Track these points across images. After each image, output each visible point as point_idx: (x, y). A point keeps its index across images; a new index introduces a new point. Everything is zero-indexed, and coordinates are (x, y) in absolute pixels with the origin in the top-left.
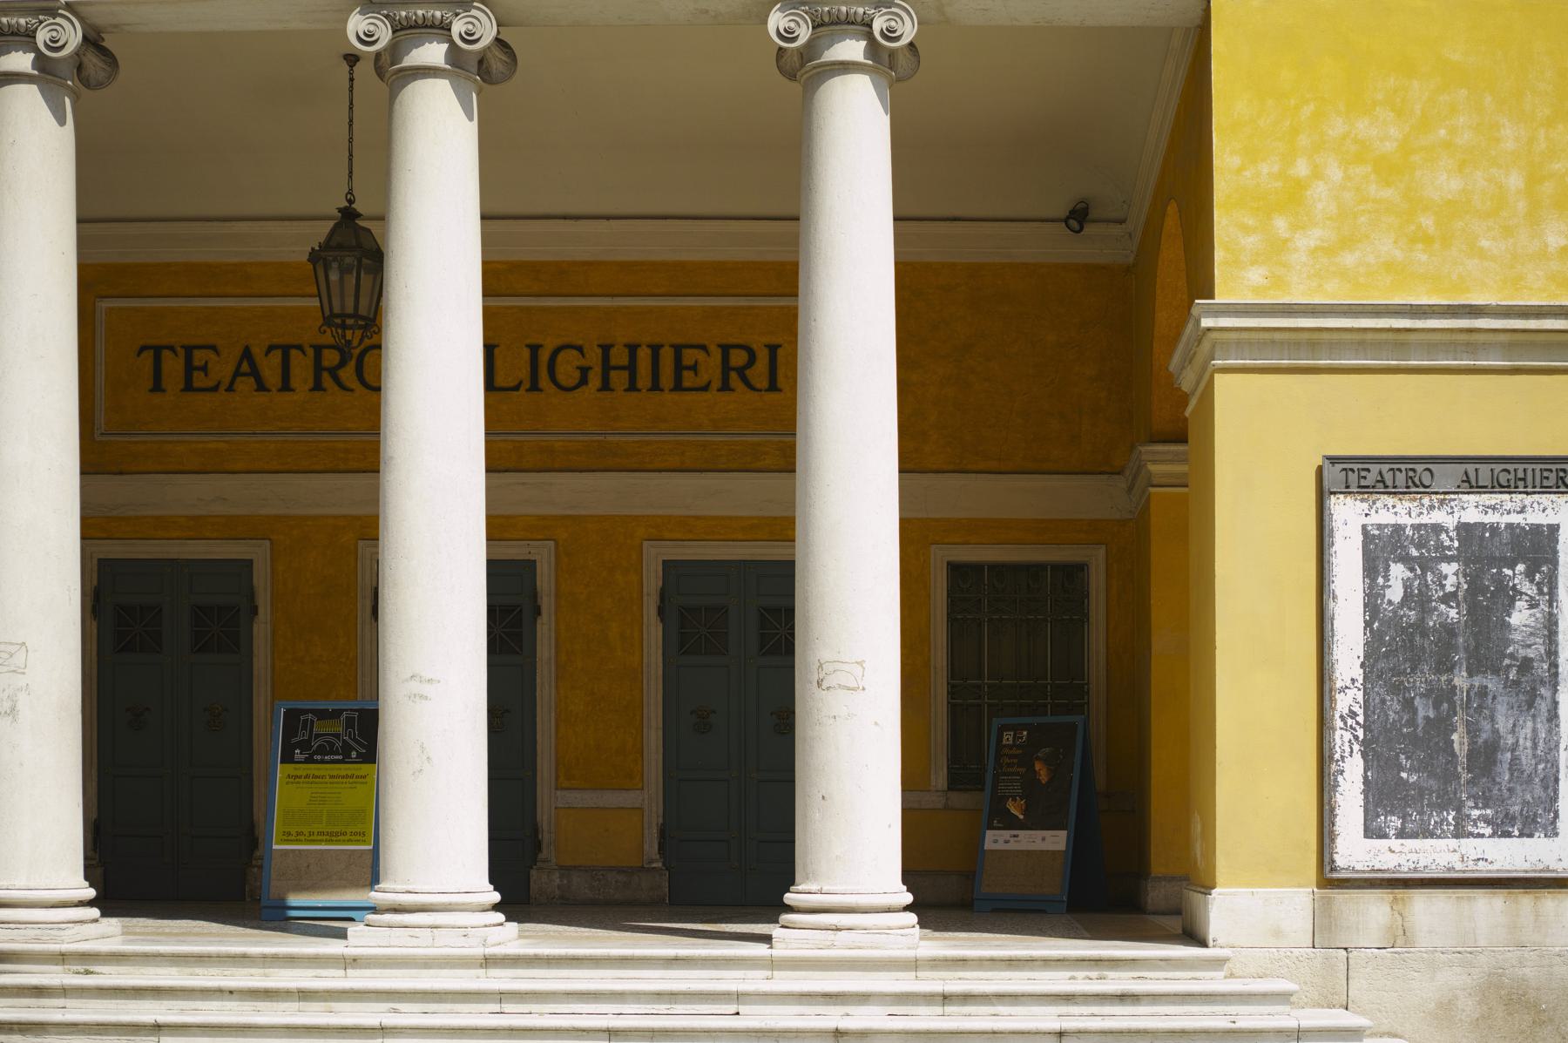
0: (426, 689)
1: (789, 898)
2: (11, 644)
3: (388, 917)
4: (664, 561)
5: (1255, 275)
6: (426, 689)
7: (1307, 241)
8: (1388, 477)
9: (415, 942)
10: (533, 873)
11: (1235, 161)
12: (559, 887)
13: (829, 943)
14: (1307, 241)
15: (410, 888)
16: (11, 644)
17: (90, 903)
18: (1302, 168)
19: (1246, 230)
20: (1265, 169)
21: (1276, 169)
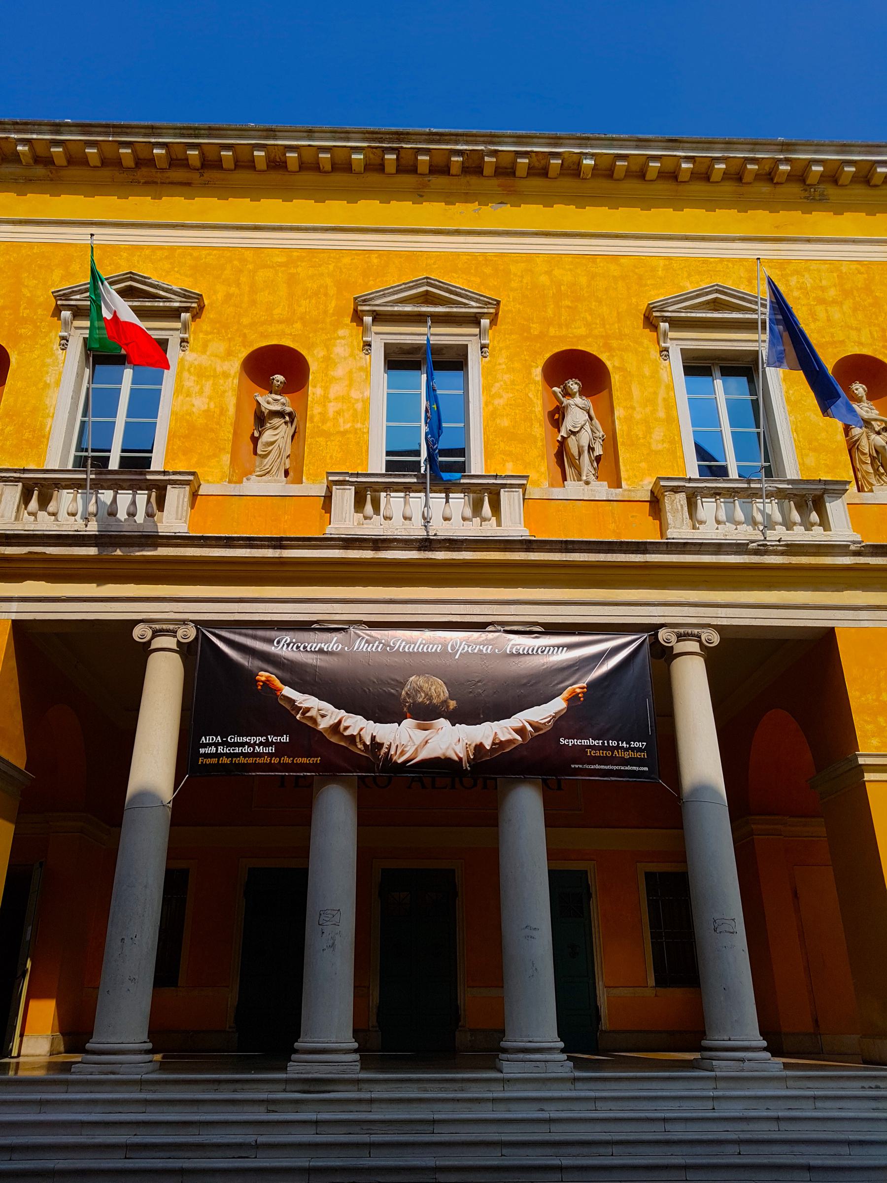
0: (535, 933)
1: (503, 1044)
2: (334, 910)
3: (521, 1056)
4: (454, 870)
5: (875, 742)
6: (535, 933)
9: (536, 1070)
10: (457, 1033)
11: (858, 694)
12: (470, 1041)
13: (741, 1068)
15: (531, 1039)
16: (334, 910)
17: (765, 1049)
19: (868, 723)
20: (869, 696)
21: (874, 697)
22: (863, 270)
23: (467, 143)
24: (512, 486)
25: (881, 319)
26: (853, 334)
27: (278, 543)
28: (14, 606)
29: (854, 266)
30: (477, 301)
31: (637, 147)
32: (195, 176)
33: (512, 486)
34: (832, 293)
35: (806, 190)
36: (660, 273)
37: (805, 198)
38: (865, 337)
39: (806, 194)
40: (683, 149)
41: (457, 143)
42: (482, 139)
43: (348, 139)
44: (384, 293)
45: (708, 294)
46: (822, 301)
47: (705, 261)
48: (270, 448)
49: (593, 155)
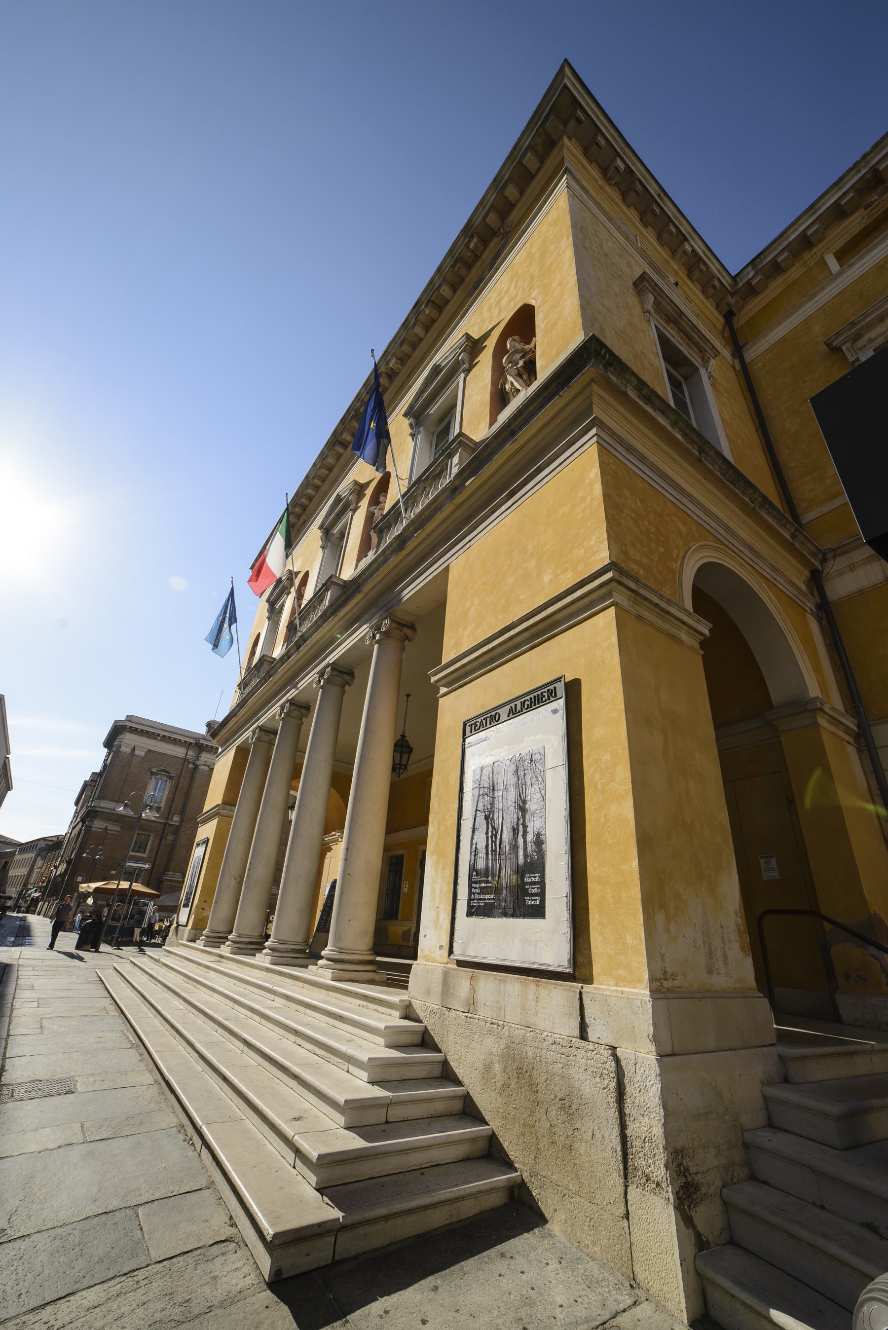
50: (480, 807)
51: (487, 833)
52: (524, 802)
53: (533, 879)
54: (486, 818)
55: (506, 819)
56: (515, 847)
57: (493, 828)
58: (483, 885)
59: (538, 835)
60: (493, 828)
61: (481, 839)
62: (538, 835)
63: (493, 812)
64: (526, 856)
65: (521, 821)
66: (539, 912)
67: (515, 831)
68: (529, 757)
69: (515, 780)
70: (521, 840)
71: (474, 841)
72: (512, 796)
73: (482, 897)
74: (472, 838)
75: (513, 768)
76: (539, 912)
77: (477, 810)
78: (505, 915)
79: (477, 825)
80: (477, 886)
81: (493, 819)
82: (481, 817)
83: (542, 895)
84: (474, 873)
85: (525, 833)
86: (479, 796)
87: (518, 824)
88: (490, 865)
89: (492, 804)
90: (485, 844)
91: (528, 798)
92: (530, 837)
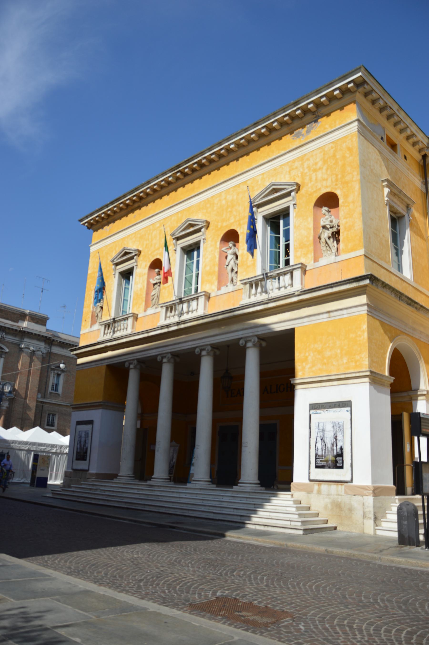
7: (308, 367)
8: (319, 407)
14: (308, 367)
18: (307, 354)
22: (333, 145)
23: (196, 158)
24: (201, 296)
25: (337, 170)
26: (325, 182)
27: (147, 331)
28: (106, 361)
29: (332, 145)
30: (201, 222)
31: (245, 132)
32: (139, 204)
33: (201, 296)
34: (320, 164)
35: (313, 115)
36: (259, 183)
37: (315, 117)
38: (329, 183)
39: (315, 116)
40: (260, 125)
41: (193, 160)
42: (199, 155)
43: (166, 174)
44: (177, 230)
45: (269, 188)
46: (315, 171)
47: (275, 169)
48: (154, 297)
49: (232, 143)
50: (319, 435)
51: (322, 444)
52: (336, 437)
53: (340, 459)
54: (322, 439)
55: (329, 441)
56: (333, 450)
57: (324, 443)
58: (321, 459)
59: (341, 447)
60: (324, 443)
61: (319, 446)
62: (341, 447)
63: (324, 438)
64: (337, 453)
65: (335, 442)
66: (342, 467)
67: (333, 445)
68: (338, 423)
69: (333, 429)
70: (335, 448)
71: (317, 446)
72: (332, 434)
73: (320, 463)
74: (316, 445)
75: (332, 425)
76: (342, 467)
77: (317, 436)
78: (329, 468)
79: (317, 441)
80: (319, 460)
81: (324, 440)
82: (319, 440)
83: (343, 463)
84: (317, 456)
85: (336, 446)
86: (318, 432)
87: (334, 443)
88: (323, 453)
89: (324, 435)
90: (321, 447)
91: (337, 436)
92: (339, 447)
